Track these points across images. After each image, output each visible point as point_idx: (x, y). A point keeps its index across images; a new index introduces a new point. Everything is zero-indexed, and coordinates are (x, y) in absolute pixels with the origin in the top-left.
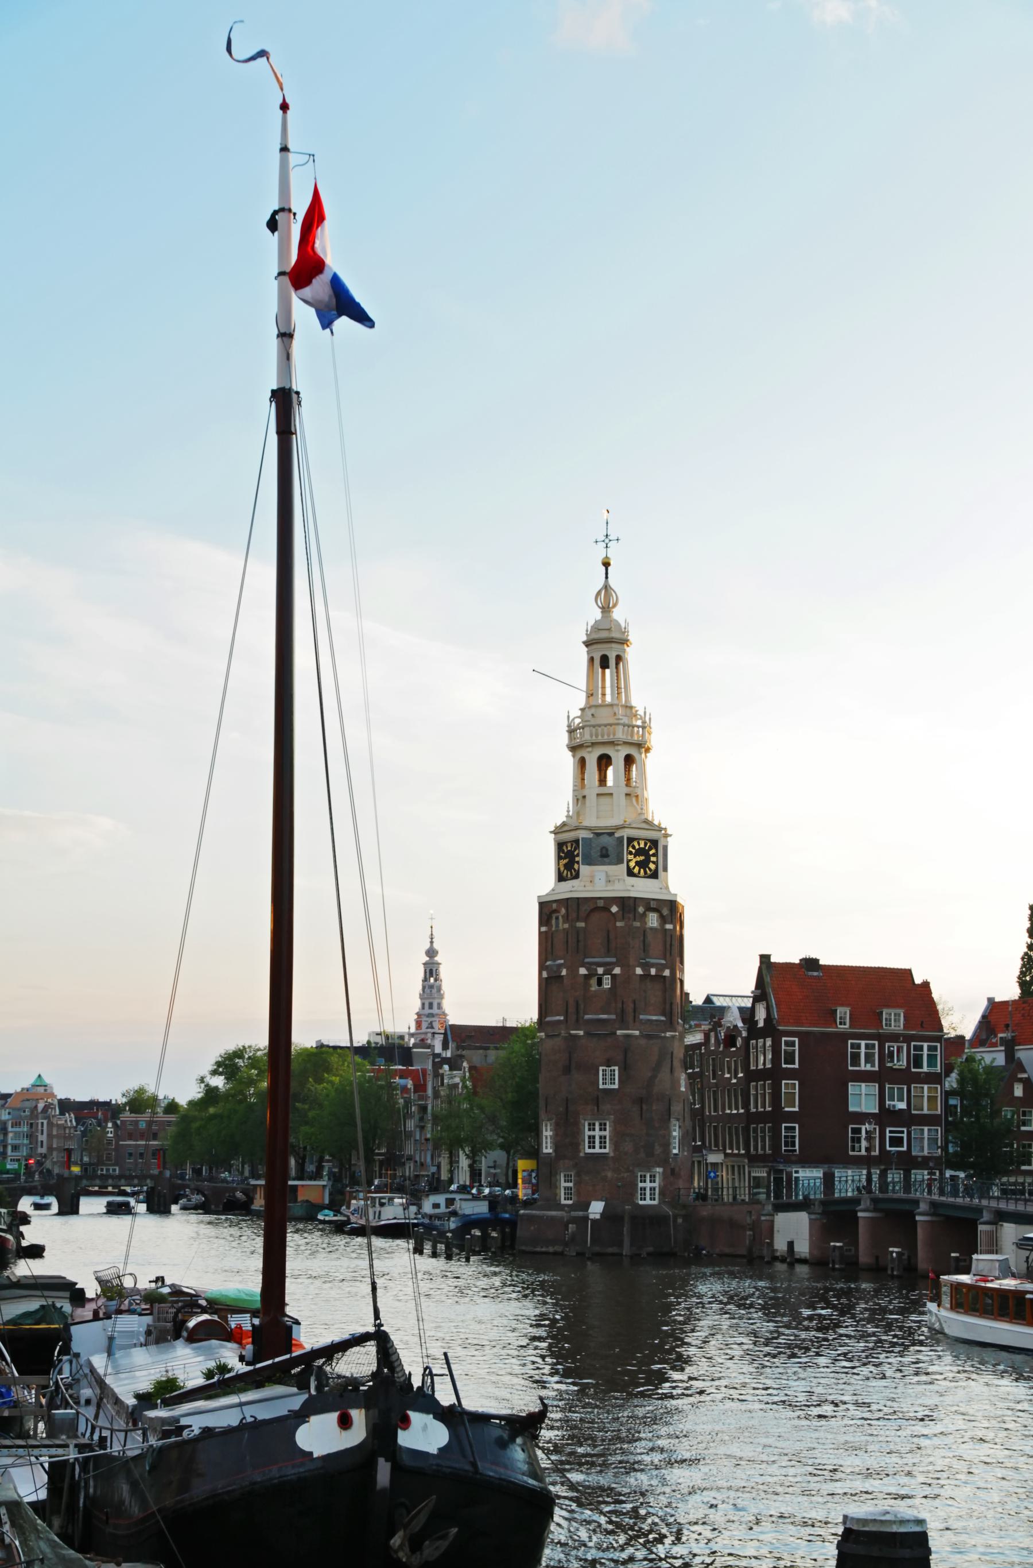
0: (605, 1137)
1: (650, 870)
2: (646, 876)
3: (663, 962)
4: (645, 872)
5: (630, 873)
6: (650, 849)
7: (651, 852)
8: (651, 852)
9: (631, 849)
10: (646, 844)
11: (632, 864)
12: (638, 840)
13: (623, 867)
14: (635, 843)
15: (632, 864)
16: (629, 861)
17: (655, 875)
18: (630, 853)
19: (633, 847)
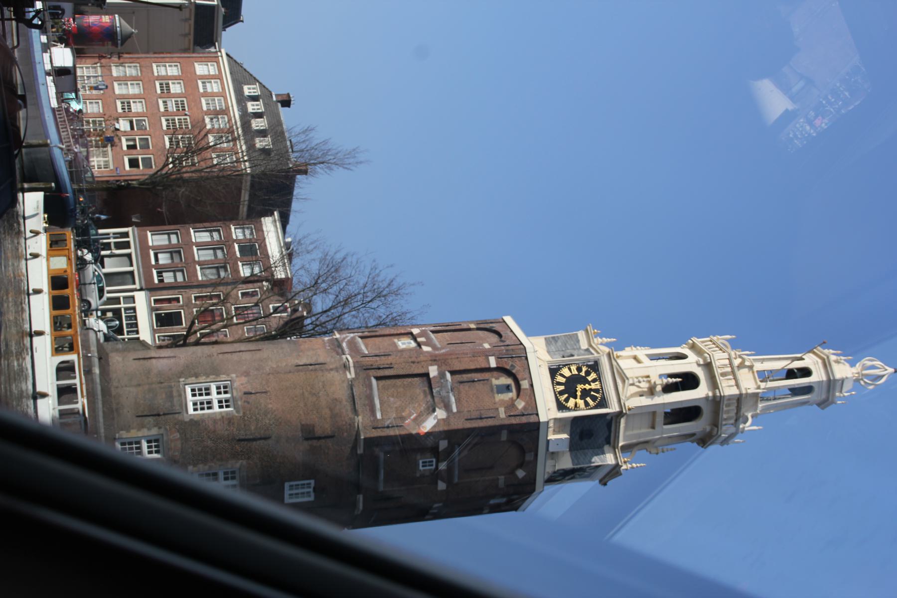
0: (209, 408)
1: (567, 400)
2: (557, 395)
3: (455, 410)
4: (561, 393)
5: (554, 372)
6: (594, 398)
7: (588, 399)
8: (588, 399)
9: (584, 369)
10: (597, 391)
11: (566, 372)
12: (599, 379)
13: (558, 359)
14: (593, 376)
15: (566, 372)
16: (568, 365)
17: (561, 407)
18: (579, 369)
19: (588, 373)
